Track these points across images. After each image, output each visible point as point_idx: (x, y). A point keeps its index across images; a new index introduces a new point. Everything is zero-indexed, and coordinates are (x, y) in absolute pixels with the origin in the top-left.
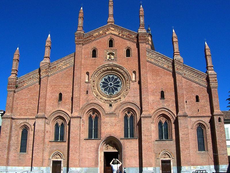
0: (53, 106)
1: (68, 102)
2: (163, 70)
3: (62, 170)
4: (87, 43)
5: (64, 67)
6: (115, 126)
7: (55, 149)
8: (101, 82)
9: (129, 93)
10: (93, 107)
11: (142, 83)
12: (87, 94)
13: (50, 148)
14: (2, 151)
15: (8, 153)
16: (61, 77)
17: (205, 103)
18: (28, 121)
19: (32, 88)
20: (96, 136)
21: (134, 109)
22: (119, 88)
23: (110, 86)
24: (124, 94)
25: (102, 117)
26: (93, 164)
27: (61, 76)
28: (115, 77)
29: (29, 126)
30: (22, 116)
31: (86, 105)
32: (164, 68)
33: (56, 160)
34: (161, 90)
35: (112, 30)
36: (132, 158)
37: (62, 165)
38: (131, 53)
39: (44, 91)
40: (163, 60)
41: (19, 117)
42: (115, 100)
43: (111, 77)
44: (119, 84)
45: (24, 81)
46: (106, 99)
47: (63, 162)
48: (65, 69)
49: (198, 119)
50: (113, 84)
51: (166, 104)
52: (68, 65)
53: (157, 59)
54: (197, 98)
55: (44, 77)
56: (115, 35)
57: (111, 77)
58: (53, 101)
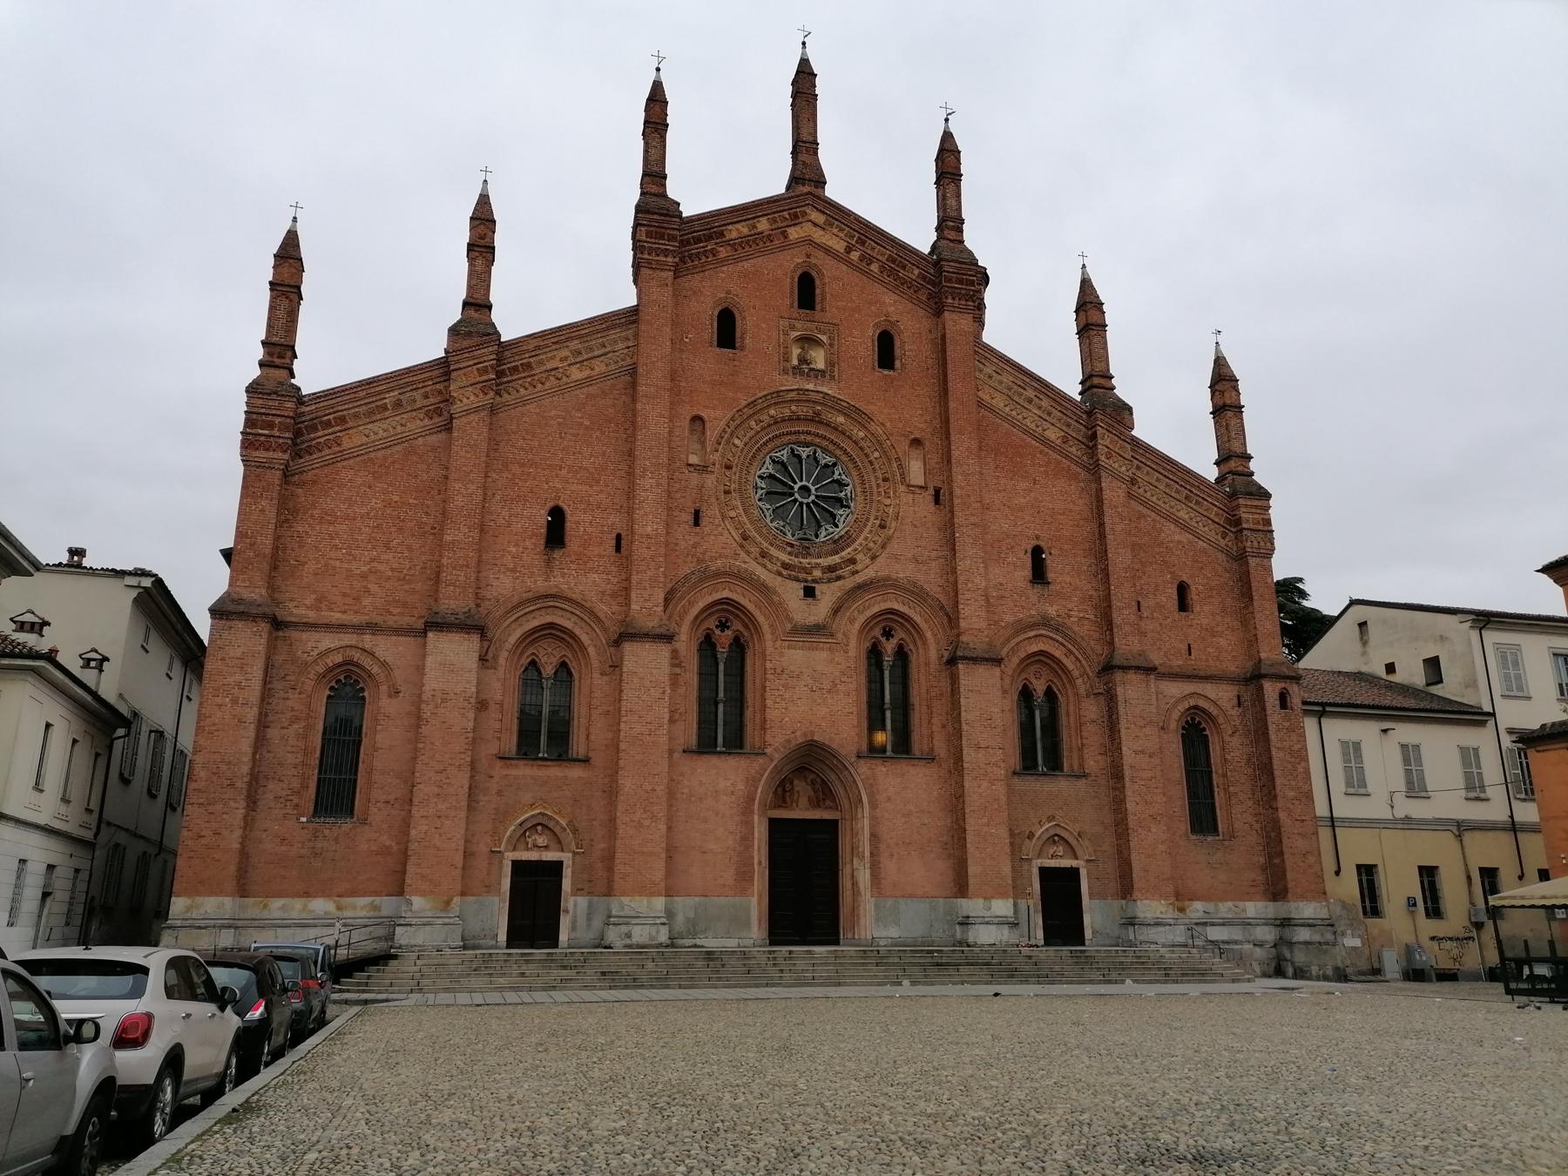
0: (514, 570)
1: (600, 556)
2: (1041, 452)
3: (567, 911)
4: (695, 267)
5: (576, 374)
6: (829, 691)
7: (527, 797)
10: (726, 594)
12: (697, 523)
13: (499, 793)
14: (211, 808)
15: (248, 823)
16: (559, 424)
17: (1218, 618)
18: (368, 640)
19: (394, 462)
20: (736, 743)
21: (917, 619)
24: (871, 545)
25: (769, 644)
26: (729, 876)
27: (559, 416)
28: (826, 459)
29: (375, 670)
30: (331, 610)
31: (694, 578)
32: (1045, 442)
33: (533, 856)
34: (1035, 542)
35: (815, 225)
36: (909, 854)
37: (567, 884)
38: (897, 352)
39: (472, 487)
40: (1045, 403)
41: (312, 616)
42: (831, 569)
44: (842, 495)
45: (343, 420)
46: (785, 557)
47: (570, 870)
48: (580, 384)
49: (1189, 687)
51: (1055, 608)
52: (599, 367)
53: (1020, 395)
54: (1182, 589)
55: (468, 412)
56: (828, 251)
57: (804, 456)
58: (517, 545)
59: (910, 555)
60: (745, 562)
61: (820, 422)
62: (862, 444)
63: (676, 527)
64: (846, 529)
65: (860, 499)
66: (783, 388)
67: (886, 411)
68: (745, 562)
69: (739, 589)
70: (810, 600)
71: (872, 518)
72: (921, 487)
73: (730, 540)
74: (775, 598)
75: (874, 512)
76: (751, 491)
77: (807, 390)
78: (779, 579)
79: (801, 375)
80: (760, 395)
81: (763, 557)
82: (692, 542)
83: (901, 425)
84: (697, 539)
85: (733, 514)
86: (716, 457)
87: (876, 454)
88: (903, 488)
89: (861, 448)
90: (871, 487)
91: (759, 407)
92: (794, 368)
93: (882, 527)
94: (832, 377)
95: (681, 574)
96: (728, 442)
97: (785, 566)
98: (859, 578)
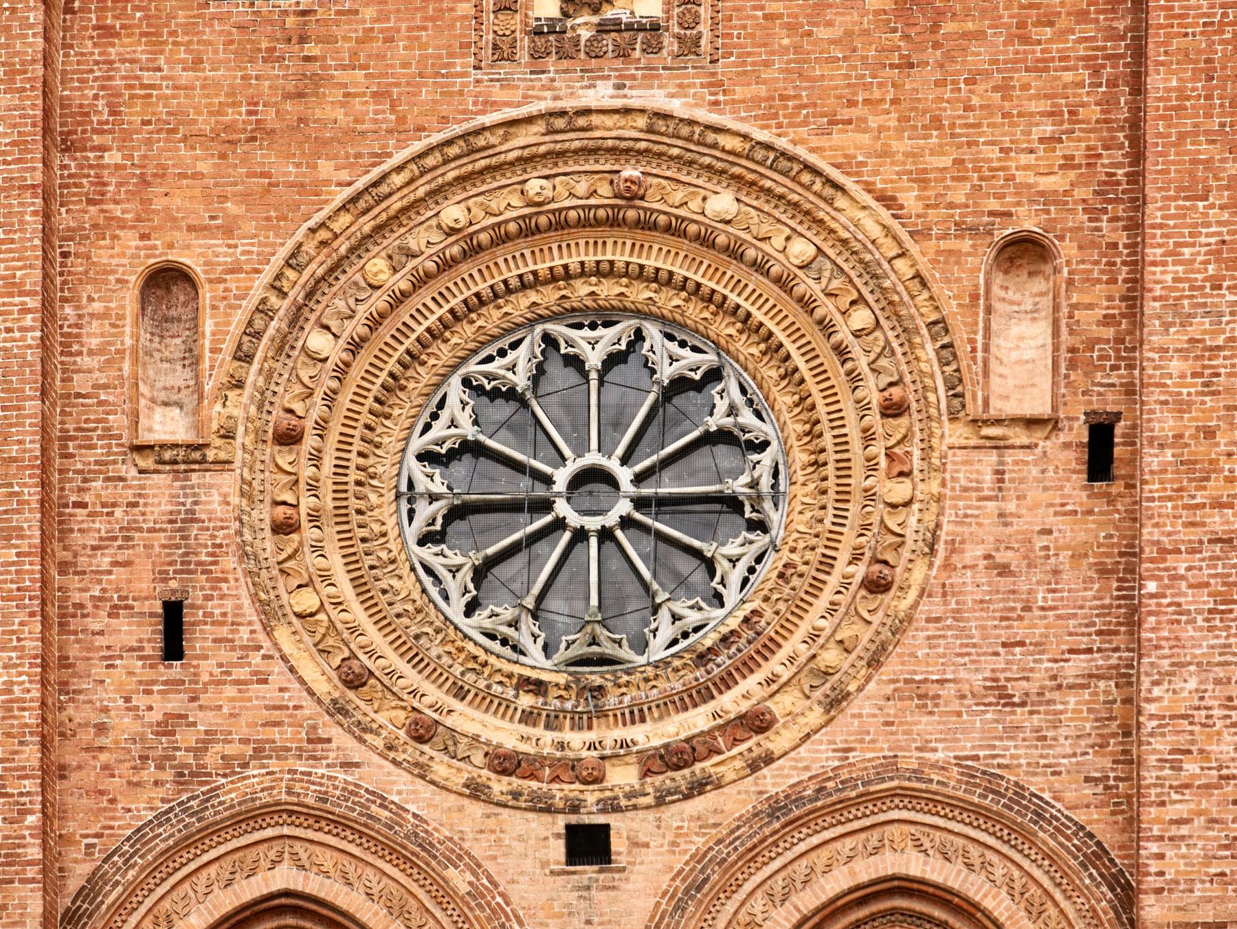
8: (418, 443)
9: (916, 638)
10: (283, 878)
11: (1153, 459)
12: (173, 648)
22: (732, 549)
23: (574, 520)
24: (831, 657)
31: (166, 837)
43: (594, 359)
50: (624, 475)
59: (978, 680)
60: (348, 765)
61: (646, 225)
62: (807, 285)
63: (98, 670)
64: (748, 607)
65: (803, 493)
66: (488, 119)
67: (901, 146)
68: (348, 765)
69: (327, 859)
70: (589, 871)
71: (843, 556)
72: (1031, 423)
73: (298, 693)
74: (460, 880)
75: (849, 538)
76: (386, 512)
77: (587, 112)
78: (476, 809)
79: (562, 55)
80: (398, 158)
81: (420, 739)
82: (156, 716)
83: (959, 195)
84: (176, 703)
85: (307, 601)
86: (239, 406)
87: (861, 318)
88: (954, 434)
89: (807, 304)
90: (842, 443)
91: (395, 203)
92: (538, 32)
93: (876, 586)
94: (690, 46)
95: (124, 826)
96: (282, 346)
97: (506, 763)
98: (774, 781)
